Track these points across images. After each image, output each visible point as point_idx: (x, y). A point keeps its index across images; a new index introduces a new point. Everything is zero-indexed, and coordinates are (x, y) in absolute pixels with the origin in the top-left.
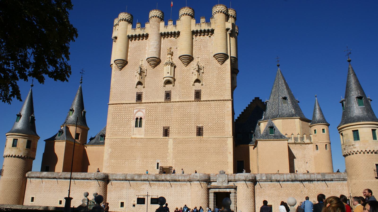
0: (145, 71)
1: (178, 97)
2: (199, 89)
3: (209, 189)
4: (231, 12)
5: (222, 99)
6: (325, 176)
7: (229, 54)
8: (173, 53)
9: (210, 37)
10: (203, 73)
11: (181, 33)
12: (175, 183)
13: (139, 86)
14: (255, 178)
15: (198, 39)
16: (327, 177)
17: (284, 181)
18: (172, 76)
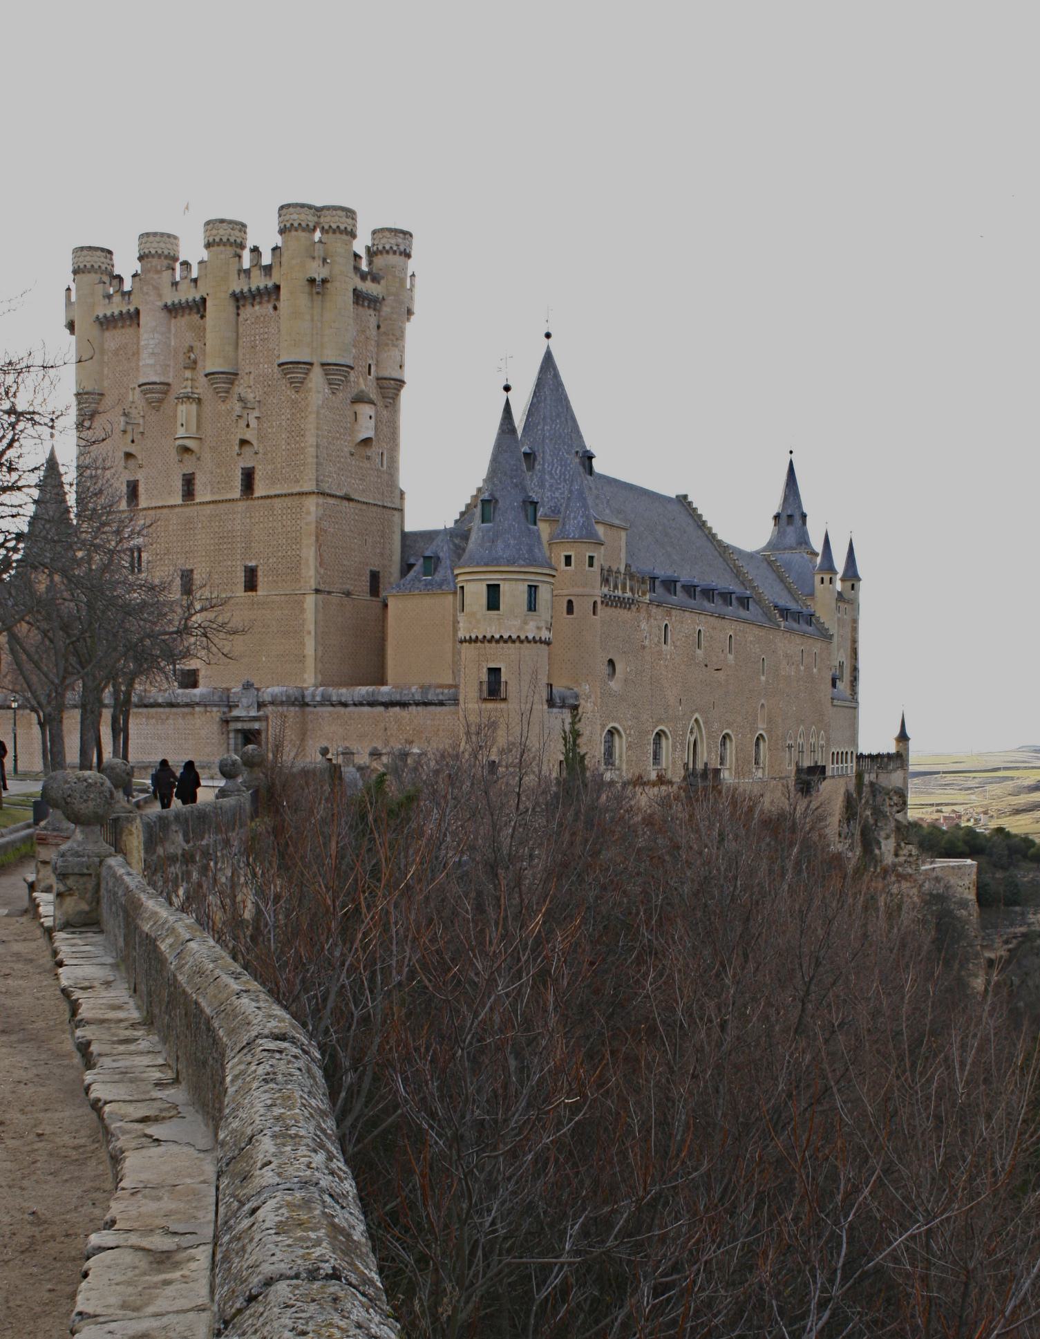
0: (141, 421)
1: (209, 488)
2: (249, 465)
3: (227, 722)
4: (328, 219)
5: (297, 489)
6: (427, 694)
7: (314, 360)
8: (195, 362)
9: (275, 308)
10: (258, 418)
11: (208, 304)
12: (174, 710)
13: (131, 462)
14: (303, 696)
15: (248, 312)
16: (430, 697)
17: (355, 705)
18: (193, 431)
